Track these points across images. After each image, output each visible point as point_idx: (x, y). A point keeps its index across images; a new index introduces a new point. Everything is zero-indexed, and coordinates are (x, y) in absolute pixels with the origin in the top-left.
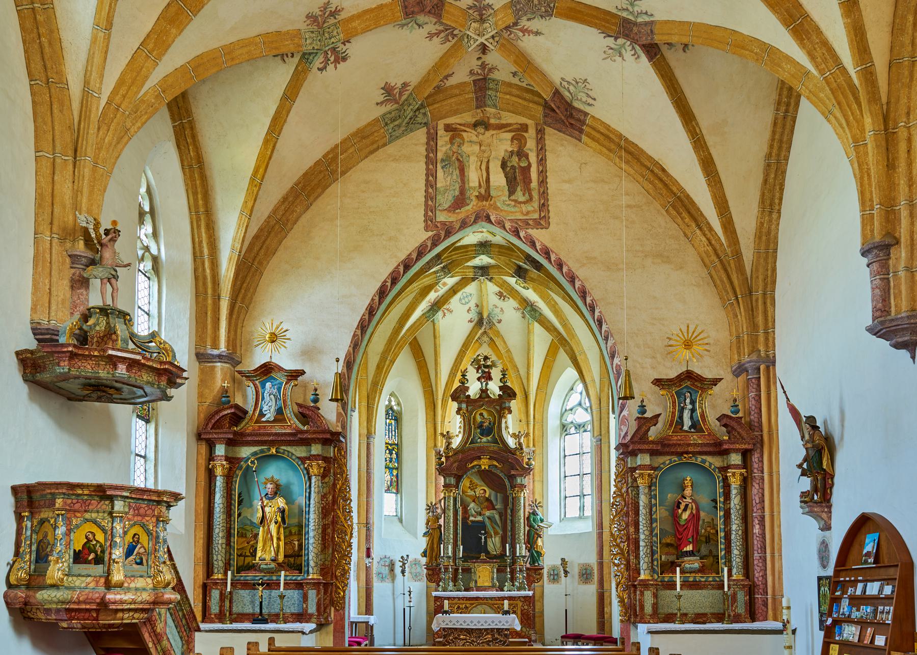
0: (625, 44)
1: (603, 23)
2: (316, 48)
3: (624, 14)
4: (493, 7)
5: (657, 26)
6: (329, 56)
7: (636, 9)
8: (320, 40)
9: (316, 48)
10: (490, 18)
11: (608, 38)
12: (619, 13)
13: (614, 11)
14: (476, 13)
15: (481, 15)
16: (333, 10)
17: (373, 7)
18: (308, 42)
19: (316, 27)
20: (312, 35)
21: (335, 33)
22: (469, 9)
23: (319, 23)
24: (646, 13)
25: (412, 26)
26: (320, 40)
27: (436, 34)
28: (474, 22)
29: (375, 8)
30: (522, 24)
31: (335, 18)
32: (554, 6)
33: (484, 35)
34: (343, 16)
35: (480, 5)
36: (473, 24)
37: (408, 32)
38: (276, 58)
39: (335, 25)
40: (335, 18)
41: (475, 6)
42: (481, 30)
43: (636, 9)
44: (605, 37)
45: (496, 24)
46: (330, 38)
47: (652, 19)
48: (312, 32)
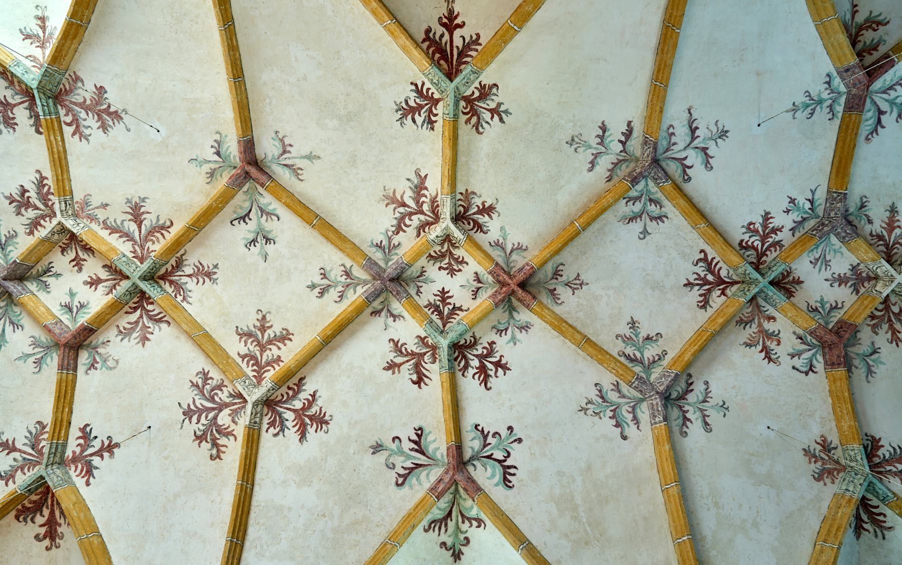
0: (887, 101)
1: (850, 131)
2: (862, 481)
3: (840, 109)
4: (855, 264)
5: (839, 65)
6: (894, 469)
7: (825, 95)
8: (856, 474)
9: (862, 481)
10: (871, 267)
11: (884, 122)
12: (840, 115)
13: (837, 122)
14: (866, 284)
15: (869, 279)
16: (819, 448)
17: (831, 401)
18: (851, 489)
19: (841, 474)
20: (846, 482)
21: (852, 453)
22: (858, 292)
23: (835, 469)
24: (829, 83)
25: (873, 361)
26: (856, 474)
27: (893, 334)
28: (875, 286)
29: (832, 399)
30: (879, 230)
31: (835, 448)
32: (836, 192)
33: (892, 276)
34: (834, 438)
35: (852, 279)
36: (877, 288)
37: (881, 366)
38: (886, 537)
39: (844, 451)
40: (835, 448)
41: (854, 284)
42: (887, 279)
43: (825, 95)
44: (883, 127)
45: (873, 260)
46: (857, 461)
47: (835, 74)
48: (844, 480)
